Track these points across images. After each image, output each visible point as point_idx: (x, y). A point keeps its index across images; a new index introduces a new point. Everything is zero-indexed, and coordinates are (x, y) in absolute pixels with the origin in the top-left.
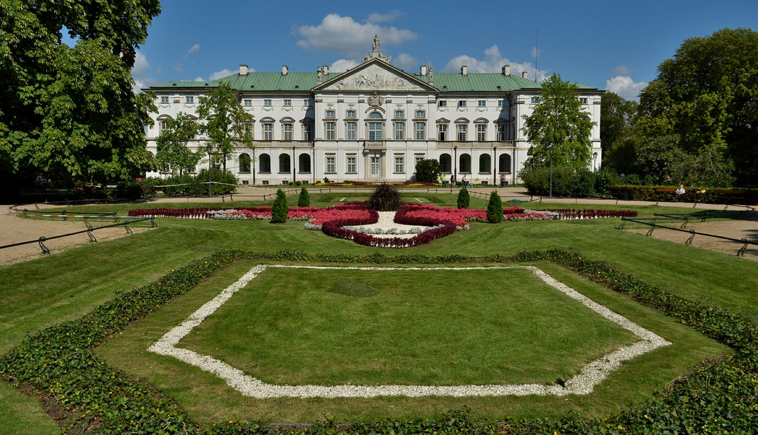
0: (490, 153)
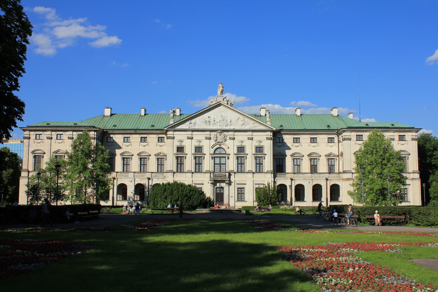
0: (323, 183)
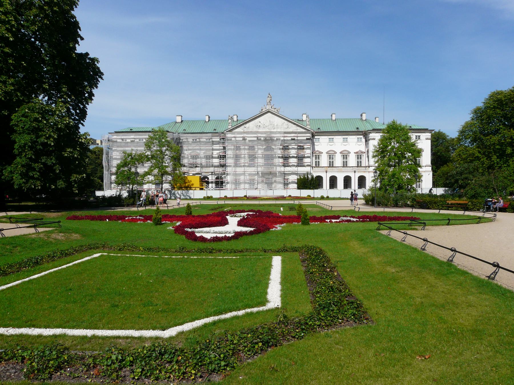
0: (351, 175)
